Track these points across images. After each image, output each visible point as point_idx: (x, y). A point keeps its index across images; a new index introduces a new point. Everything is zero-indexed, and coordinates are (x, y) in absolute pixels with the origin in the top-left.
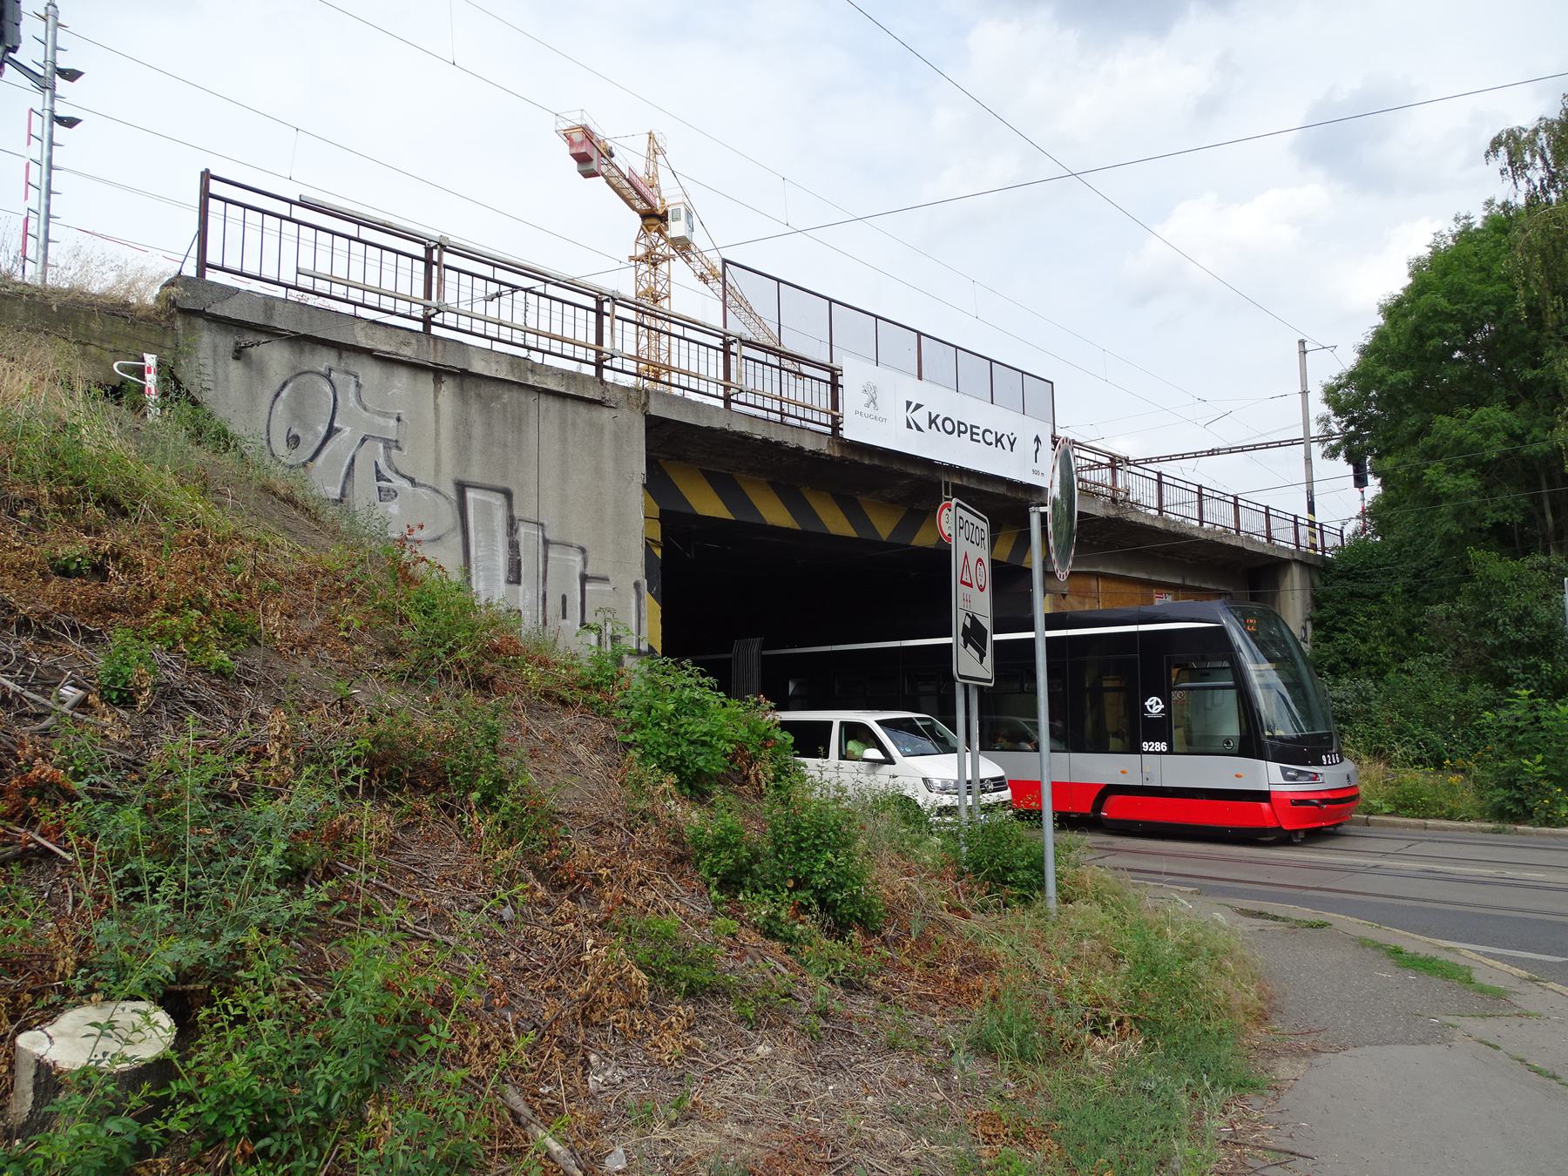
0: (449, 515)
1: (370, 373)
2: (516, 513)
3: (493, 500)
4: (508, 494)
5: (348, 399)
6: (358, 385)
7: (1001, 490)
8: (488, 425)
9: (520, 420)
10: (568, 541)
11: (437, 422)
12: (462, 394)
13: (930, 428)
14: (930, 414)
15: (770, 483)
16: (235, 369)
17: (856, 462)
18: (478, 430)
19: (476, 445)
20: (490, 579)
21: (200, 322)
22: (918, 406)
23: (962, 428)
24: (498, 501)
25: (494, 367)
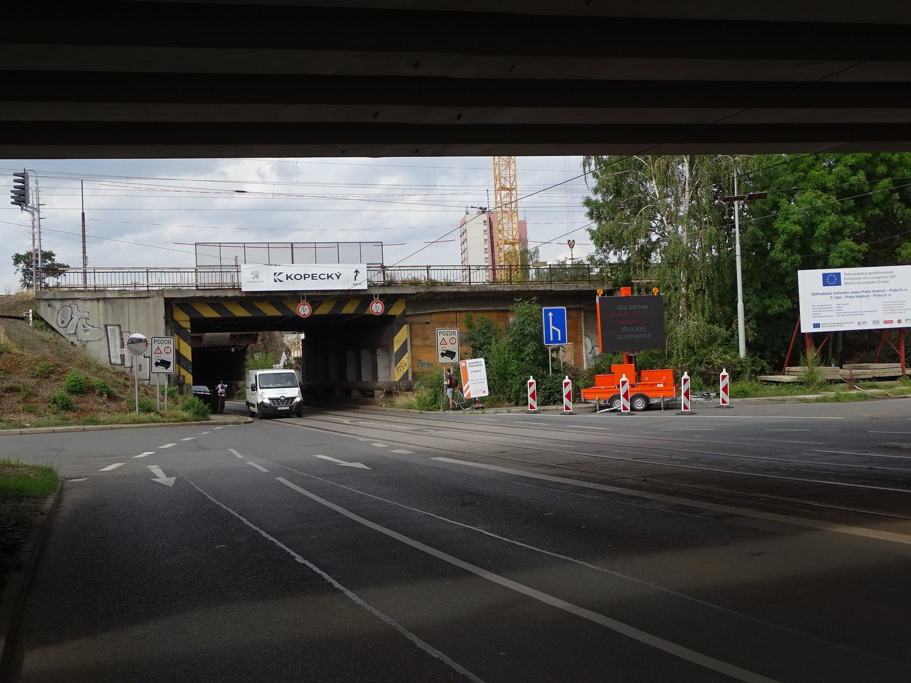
0: (103, 333)
1: (80, 303)
2: (122, 330)
4: (120, 326)
5: (75, 310)
6: (77, 306)
7: (340, 293)
8: (113, 310)
9: (122, 307)
11: (98, 311)
12: (106, 304)
13: (287, 279)
14: (287, 275)
15: (237, 303)
16: (49, 309)
17: (254, 296)
18: (110, 311)
19: (110, 315)
20: (115, 348)
21: (41, 300)
22: (280, 273)
23: (307, 276)
24: (117, 328)
25: (113, 295)
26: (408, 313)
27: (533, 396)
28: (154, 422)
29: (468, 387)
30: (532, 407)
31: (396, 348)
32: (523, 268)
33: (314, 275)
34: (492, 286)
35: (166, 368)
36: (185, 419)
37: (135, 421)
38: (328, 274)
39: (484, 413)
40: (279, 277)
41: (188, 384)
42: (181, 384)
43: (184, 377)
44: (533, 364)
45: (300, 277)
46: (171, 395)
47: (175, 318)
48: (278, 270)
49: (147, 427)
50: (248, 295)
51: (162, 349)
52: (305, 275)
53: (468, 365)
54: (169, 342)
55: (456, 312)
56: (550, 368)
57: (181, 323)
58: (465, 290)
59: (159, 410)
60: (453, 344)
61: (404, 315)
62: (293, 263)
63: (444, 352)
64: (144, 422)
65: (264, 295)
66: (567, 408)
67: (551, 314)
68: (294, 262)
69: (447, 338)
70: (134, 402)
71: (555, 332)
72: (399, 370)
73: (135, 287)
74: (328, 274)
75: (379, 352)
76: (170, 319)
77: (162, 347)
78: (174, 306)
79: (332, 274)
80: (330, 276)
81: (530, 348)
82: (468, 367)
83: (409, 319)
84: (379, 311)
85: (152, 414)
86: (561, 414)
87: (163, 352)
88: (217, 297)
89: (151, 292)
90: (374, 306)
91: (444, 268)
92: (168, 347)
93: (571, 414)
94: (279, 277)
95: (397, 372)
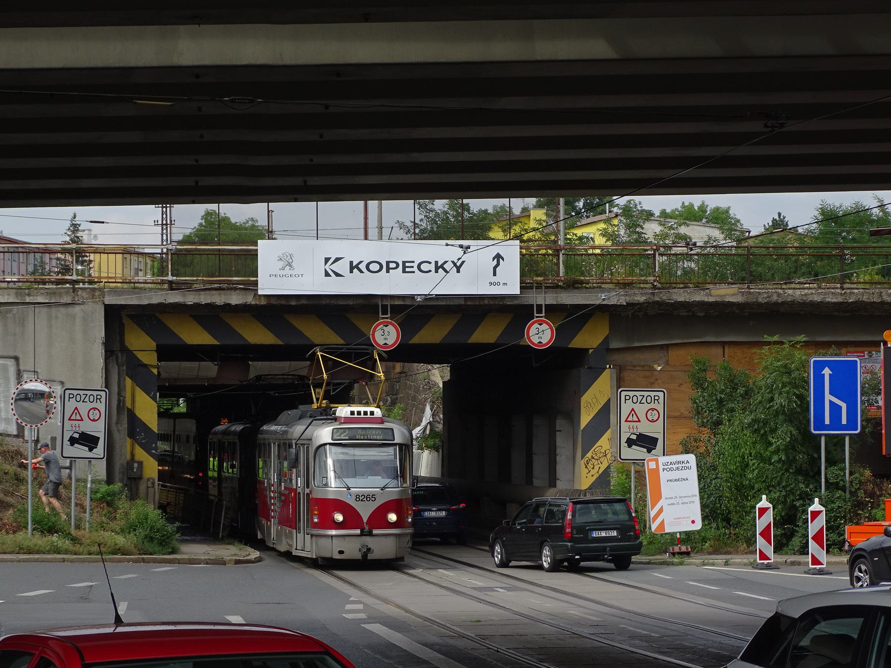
2: (22, 368)
3: (8, 363)
4: (16, 359)
9: (24, 320)
10: (53, 379)
13: (351, 272)
14: (351, 263)
17: (284, 305)
22: (337, 260)
23: (392, 265)
26: (614, 345)
27: (765, 534)
28: (58, 551)
29: (661, 511)
30: (763, 556)
31: (585, 419)
33: (407, 264)
34: (798, 292)
35: (91, 450)
36: (119, 549)
37: (21, 549)
38: (436, 262)
39: (681, 564)
40: (335, 267)
41: (148, 479)
42: (135, 479)
43: (141, 464)
44: (787, 470)
45: (372, 267)
46: (107, 502)
47: (127, 344)
48: (333, 248)
49: (36, 560)
50: (273, 302)
52: (388, 263)
53: (661, 467)
54: (98, 399)
55: (723, 344)
56: (823, 480)
57: (140, 356)
59: (73, 531)
60: (653, 421)
61: (605, 349)
62: (366, 238)
63: (634, 437)
64: (38, 552)
65: (304, 302)
66: (815, 561)
67: (827, 372)
68: (370, 238)
69: (641, 409)
70: (26, 511)
71: (835, 409)
72: (590, 466)
74: (436, 262)
75: (560, 423)
76: (116, 347)
77: (84, 408)
78: (127, 322)
79: (446, 262)
80: (442, 267)
81: (783, 435)
82: (661, 470)
83: (619, 358)
84: (545, 340)
85: (55, 538)
86: (805, 573)
88: (210, 306)
89: (80, 293)
90: (533, 330)
92: (95, 409)
93: (821, 572)
94: (335, 267)
95: (584, 471)
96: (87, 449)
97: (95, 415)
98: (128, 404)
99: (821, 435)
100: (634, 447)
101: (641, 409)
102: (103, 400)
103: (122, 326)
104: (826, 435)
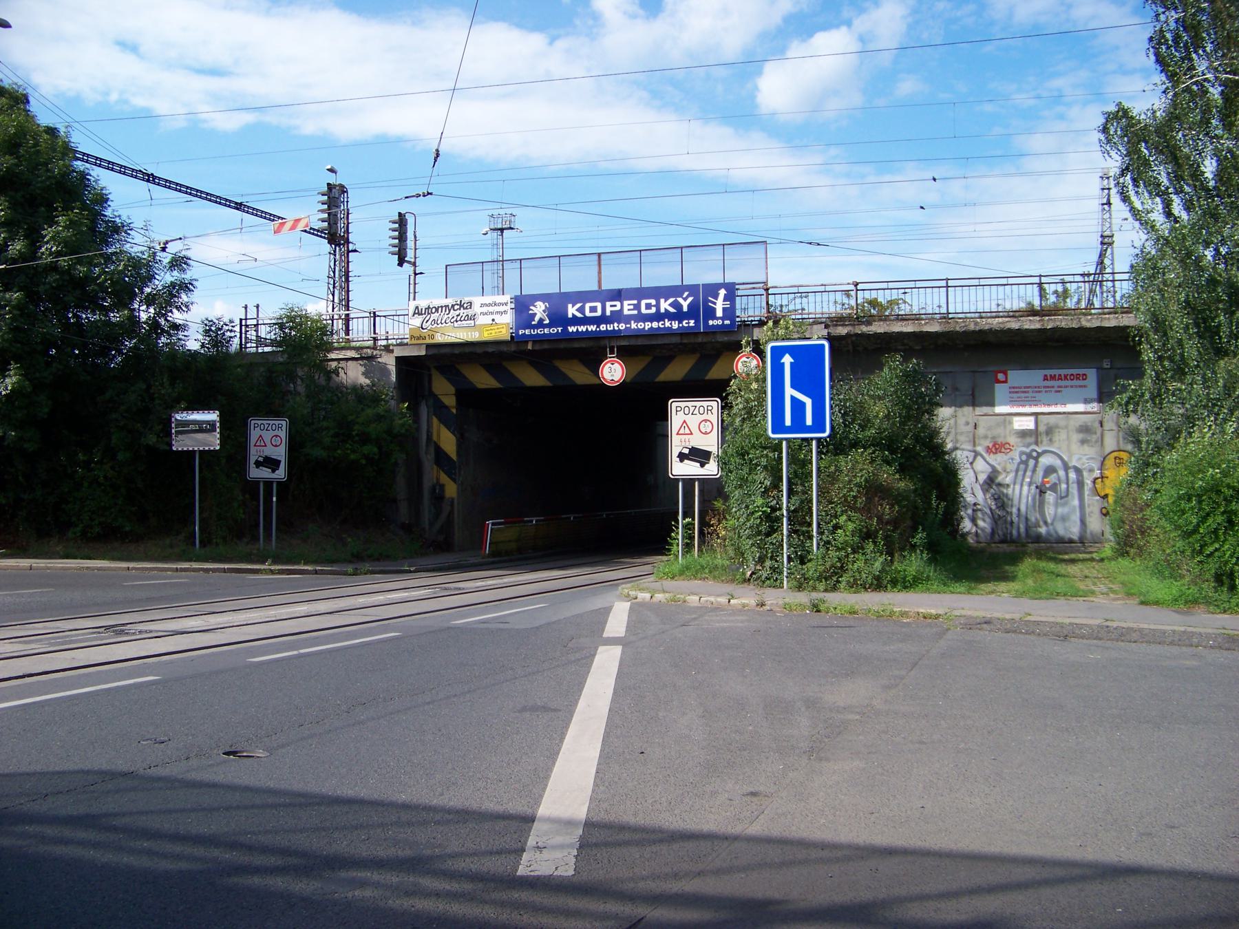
32: (1086, 279)
35: (273, 471)
51: (267, 440)
58: (934, 328)
60: (706, 433)
63: (686, 451)
65: (546, 346)
67: (787, 360)
69: (693, 421)
71: (798, 406)
73: (387, 339)
87: (268, 444)
91: (891, 285)
92: (276, 436)
96: (270, 470)
97: (277, 441)
98: (435, 438)
99: (812, 439)
100: (686, 461)
101: (693, 421)
102: (284, 428)
103: (430, 376)
104: (786, 439)
